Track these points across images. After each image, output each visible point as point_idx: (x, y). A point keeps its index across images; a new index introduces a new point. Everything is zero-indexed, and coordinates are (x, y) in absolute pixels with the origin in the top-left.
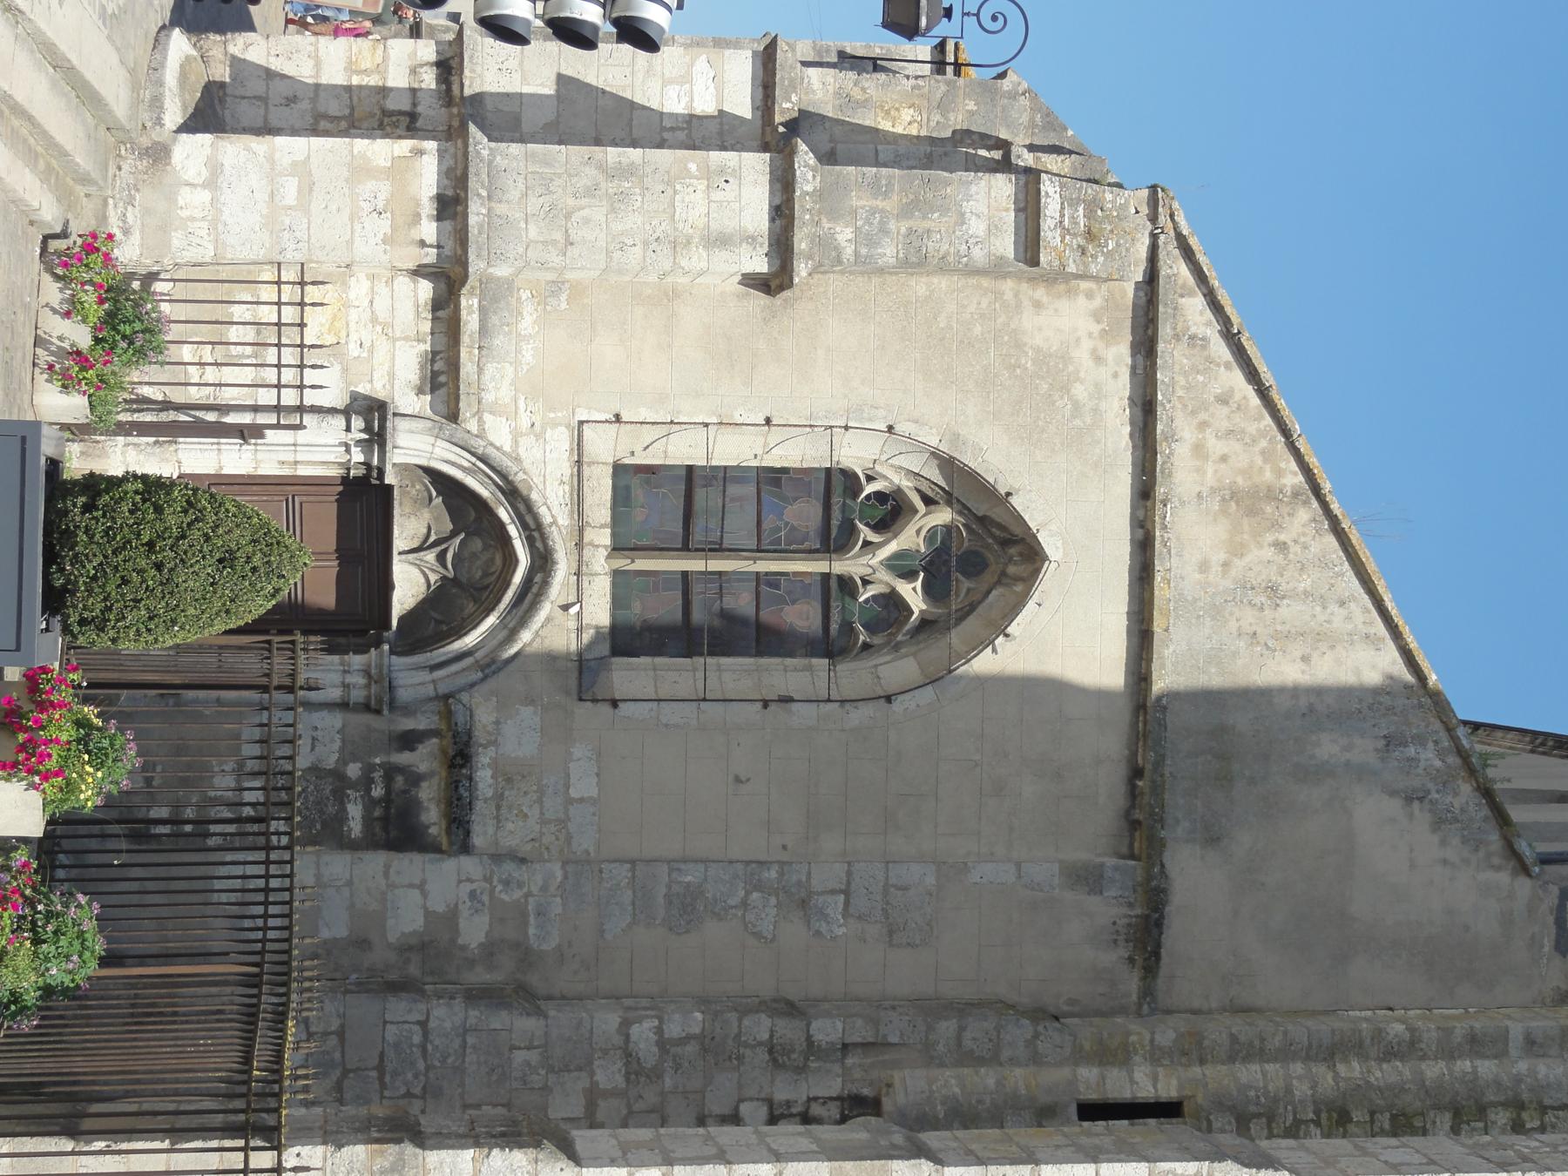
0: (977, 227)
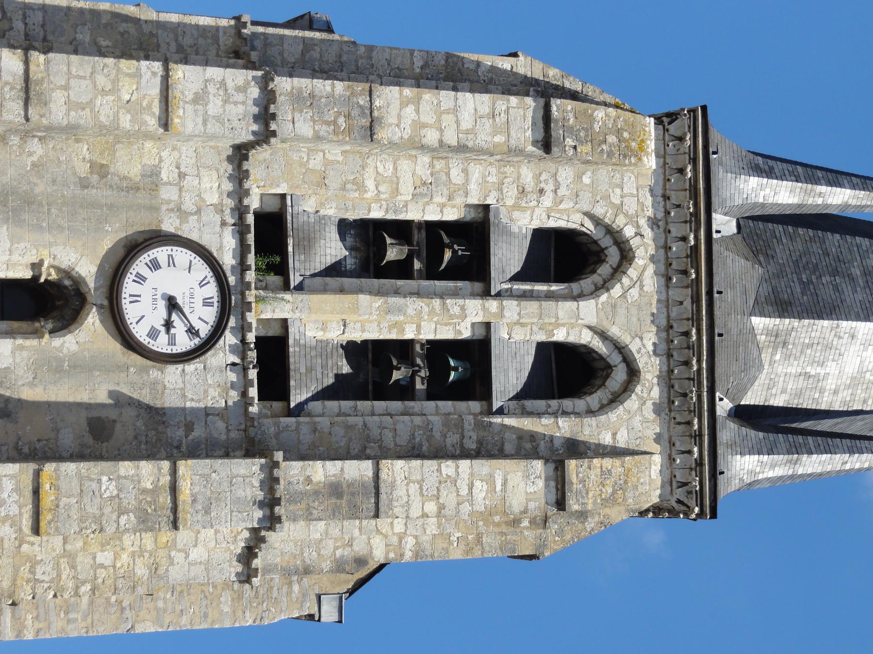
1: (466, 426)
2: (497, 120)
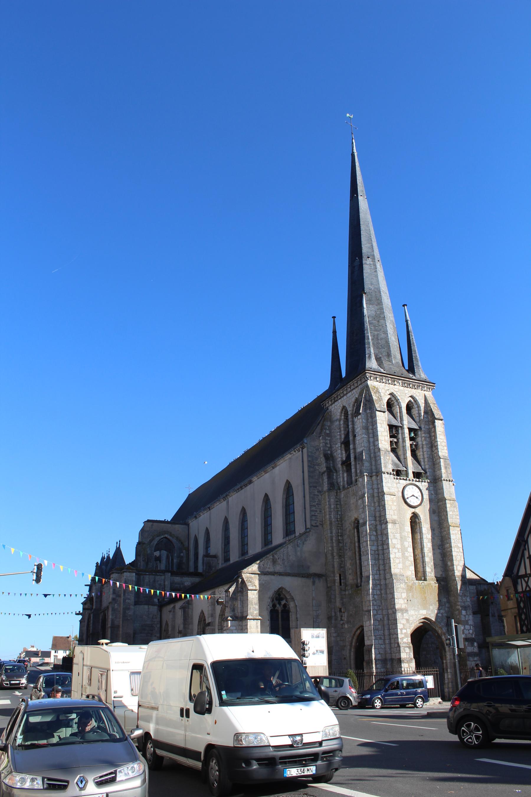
0: (254, 597)
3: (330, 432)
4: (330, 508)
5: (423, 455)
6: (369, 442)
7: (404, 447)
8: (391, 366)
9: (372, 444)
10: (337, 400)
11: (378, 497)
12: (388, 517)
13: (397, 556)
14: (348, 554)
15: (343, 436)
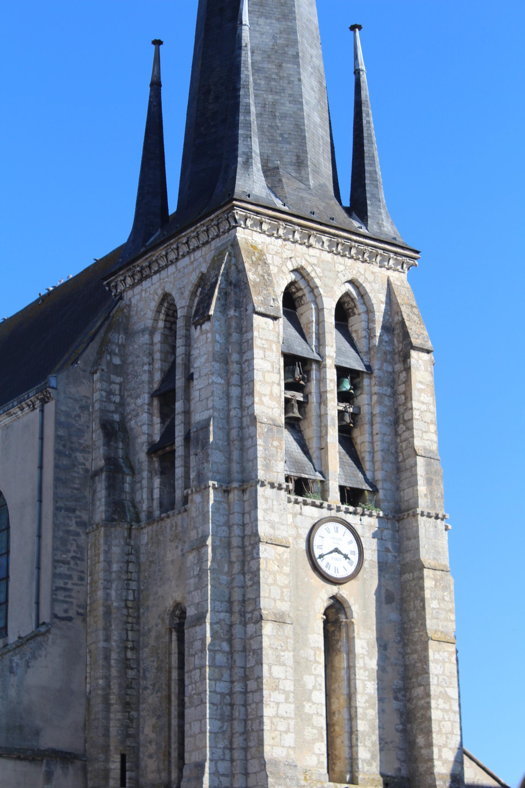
1: (381, 391)
2: (265, 346)
3: (124, 361)
4: (108, 570)
5: (372, 443)
6: (228, 396)
7: (322, 417)
8: (305, 195)
9: (234, 404)
10: (149, 276)
11: (243, 548)
12: (264, 603)
13: (282, 712)
14: (150, 700)
15: (158, 377)
